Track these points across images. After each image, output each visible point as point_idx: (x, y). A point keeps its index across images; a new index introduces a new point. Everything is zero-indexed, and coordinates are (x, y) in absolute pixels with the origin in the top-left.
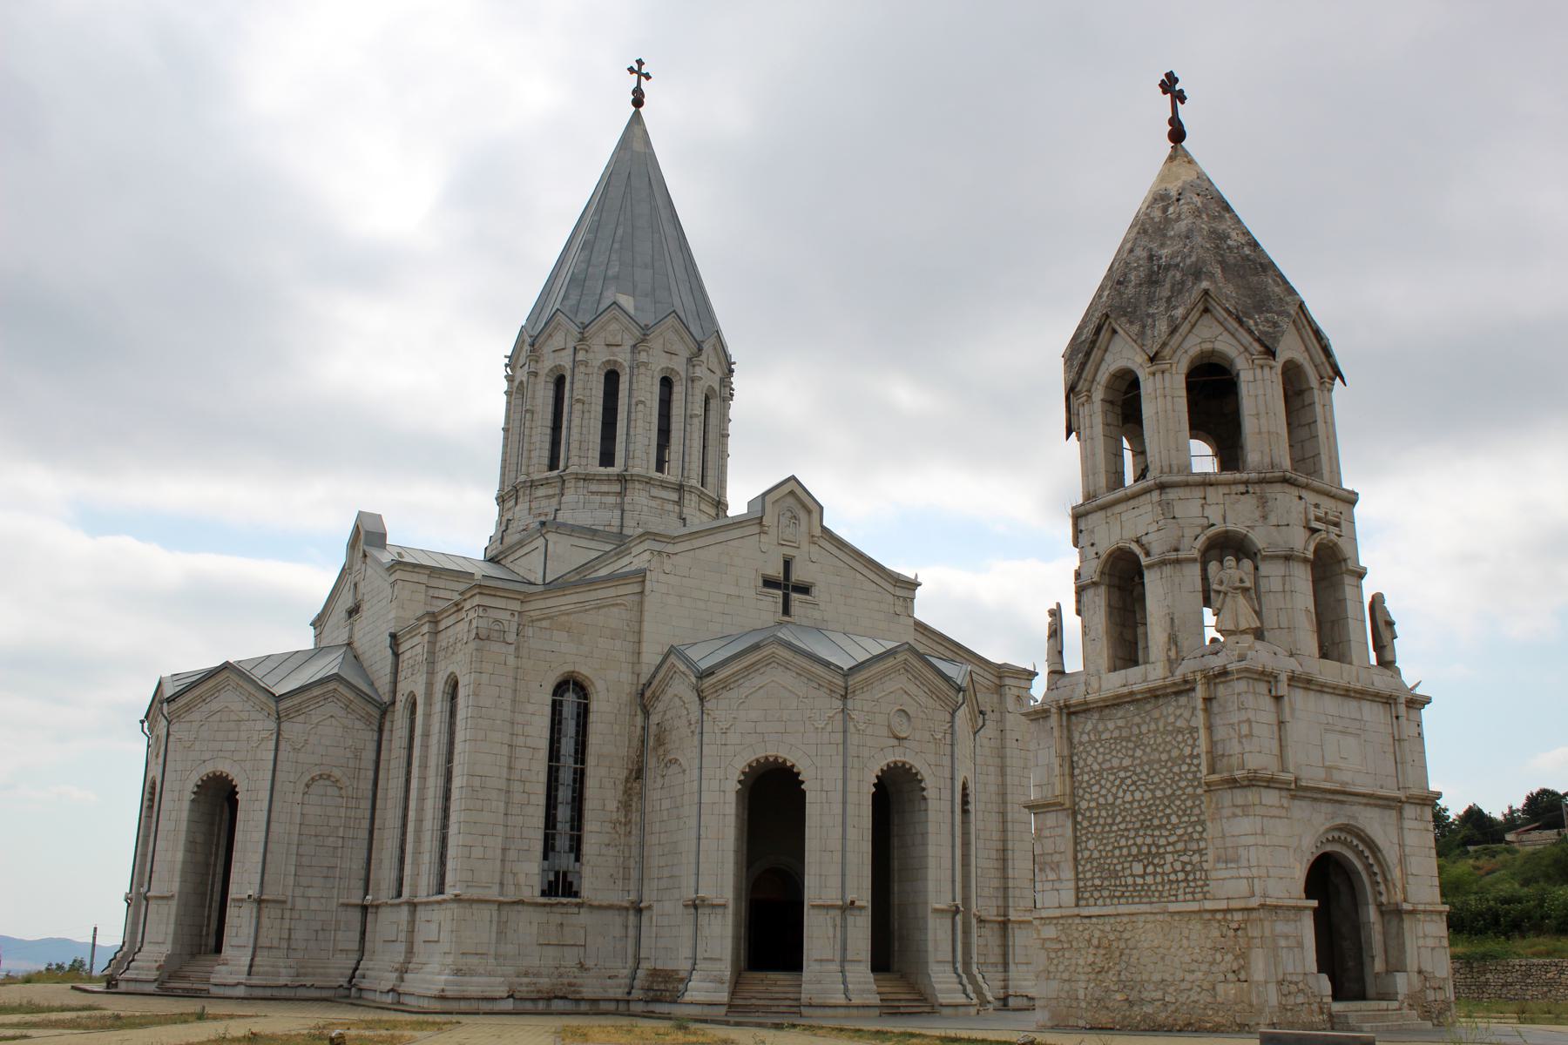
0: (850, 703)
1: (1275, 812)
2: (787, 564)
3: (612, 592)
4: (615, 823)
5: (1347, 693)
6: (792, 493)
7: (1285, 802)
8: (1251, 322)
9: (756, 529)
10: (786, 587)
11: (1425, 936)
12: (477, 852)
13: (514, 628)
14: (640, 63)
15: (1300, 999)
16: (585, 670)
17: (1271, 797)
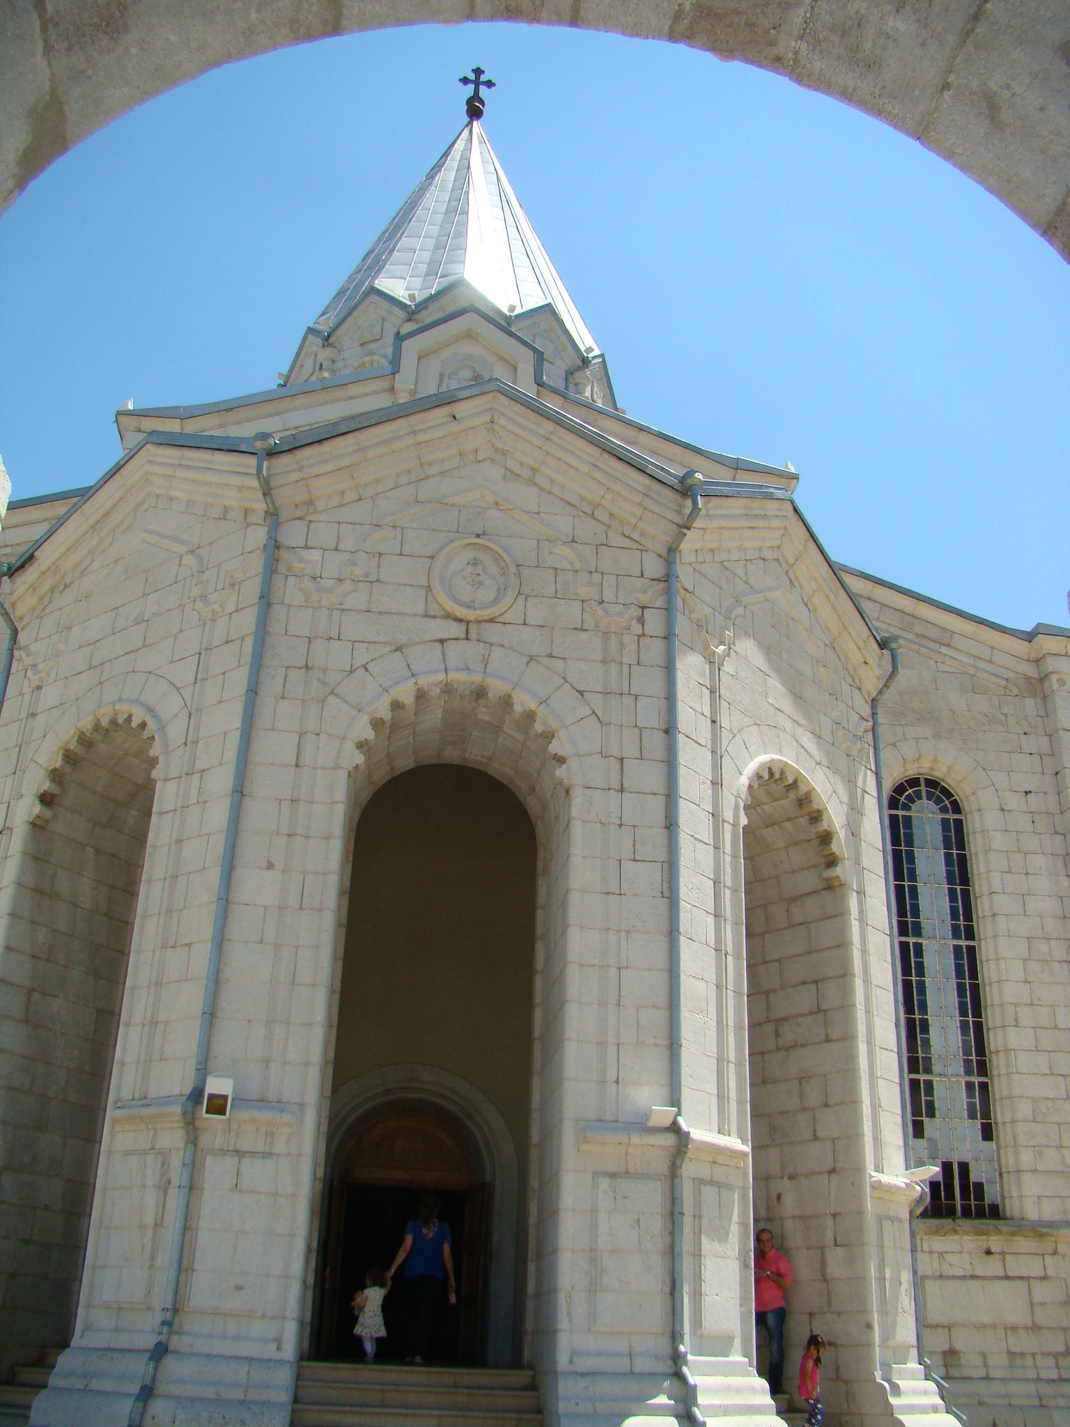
0: (292, 534)
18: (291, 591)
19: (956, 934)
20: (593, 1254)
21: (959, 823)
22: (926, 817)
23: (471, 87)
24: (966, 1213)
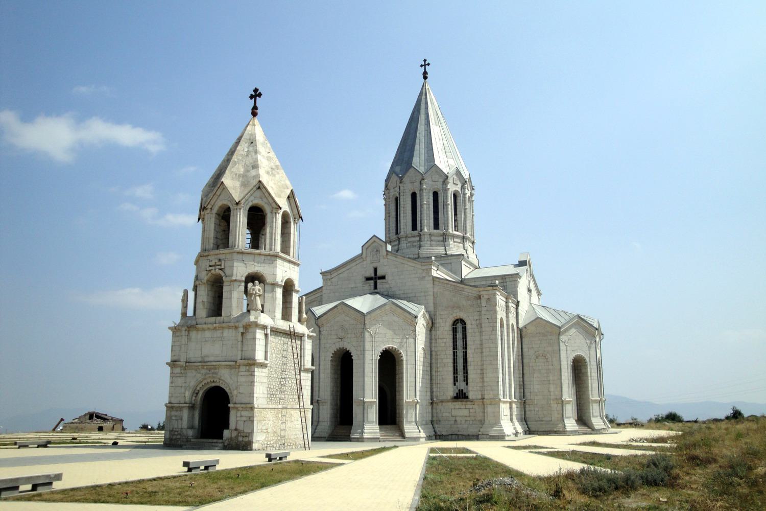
0: (321, 329)
1: (178, 375)
2: (376, 270)
3: (314, 297)
6: (375, 241)
7: (183, 371)
8: (205, 198)
9: (361, 260)
10: (376, 278)
11: (241, 416)
14: (425, 61)
15: (178, 437)
18: (322, 337)
19: (463, 349)
20: (356, 414)
21: (465, 327)
22: (459, 326)
23: (424, 67)
24: (462, 398)
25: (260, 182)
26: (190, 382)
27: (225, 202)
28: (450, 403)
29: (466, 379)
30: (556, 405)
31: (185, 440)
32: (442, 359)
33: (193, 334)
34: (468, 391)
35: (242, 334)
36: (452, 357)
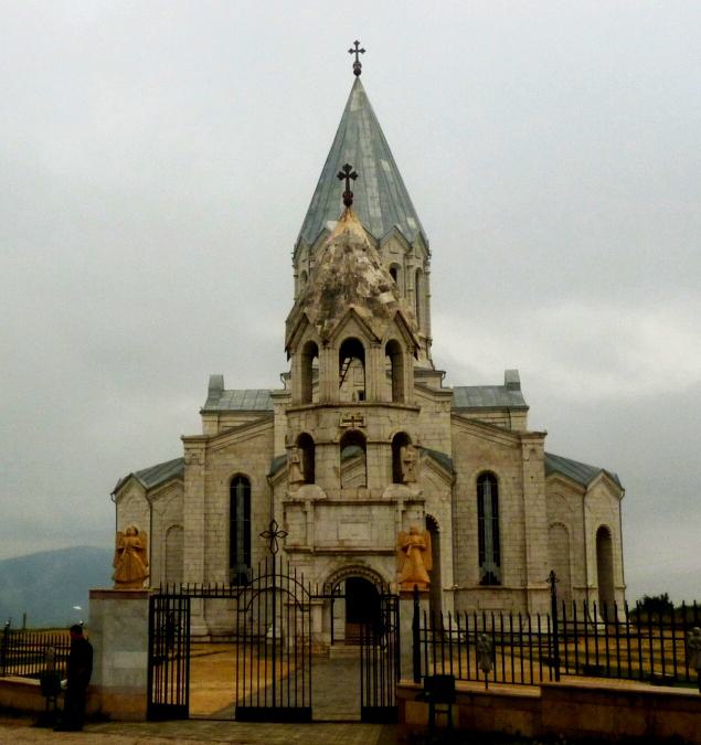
3: (256, 429)
4: (265, 548)
5: (358, 504)
7: (309, 559)
8: (320, 327)
12: (192, 567)
13: (203, 456)
16: (244, 471)
17: (299, 557)
22: (487, 485)
23: (359, 48)
25: (398, 312)
26: (320, 574)
27: (353, 335)
28: (476, 592)
29: (497, 559)
30: (577, 594)
31: (319, 648)
32: (464, 530)
33: (323, 510)
34: (501, 575)
35: (403, 512)
36: (476, 527)
